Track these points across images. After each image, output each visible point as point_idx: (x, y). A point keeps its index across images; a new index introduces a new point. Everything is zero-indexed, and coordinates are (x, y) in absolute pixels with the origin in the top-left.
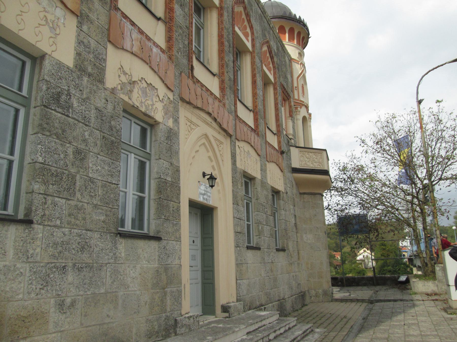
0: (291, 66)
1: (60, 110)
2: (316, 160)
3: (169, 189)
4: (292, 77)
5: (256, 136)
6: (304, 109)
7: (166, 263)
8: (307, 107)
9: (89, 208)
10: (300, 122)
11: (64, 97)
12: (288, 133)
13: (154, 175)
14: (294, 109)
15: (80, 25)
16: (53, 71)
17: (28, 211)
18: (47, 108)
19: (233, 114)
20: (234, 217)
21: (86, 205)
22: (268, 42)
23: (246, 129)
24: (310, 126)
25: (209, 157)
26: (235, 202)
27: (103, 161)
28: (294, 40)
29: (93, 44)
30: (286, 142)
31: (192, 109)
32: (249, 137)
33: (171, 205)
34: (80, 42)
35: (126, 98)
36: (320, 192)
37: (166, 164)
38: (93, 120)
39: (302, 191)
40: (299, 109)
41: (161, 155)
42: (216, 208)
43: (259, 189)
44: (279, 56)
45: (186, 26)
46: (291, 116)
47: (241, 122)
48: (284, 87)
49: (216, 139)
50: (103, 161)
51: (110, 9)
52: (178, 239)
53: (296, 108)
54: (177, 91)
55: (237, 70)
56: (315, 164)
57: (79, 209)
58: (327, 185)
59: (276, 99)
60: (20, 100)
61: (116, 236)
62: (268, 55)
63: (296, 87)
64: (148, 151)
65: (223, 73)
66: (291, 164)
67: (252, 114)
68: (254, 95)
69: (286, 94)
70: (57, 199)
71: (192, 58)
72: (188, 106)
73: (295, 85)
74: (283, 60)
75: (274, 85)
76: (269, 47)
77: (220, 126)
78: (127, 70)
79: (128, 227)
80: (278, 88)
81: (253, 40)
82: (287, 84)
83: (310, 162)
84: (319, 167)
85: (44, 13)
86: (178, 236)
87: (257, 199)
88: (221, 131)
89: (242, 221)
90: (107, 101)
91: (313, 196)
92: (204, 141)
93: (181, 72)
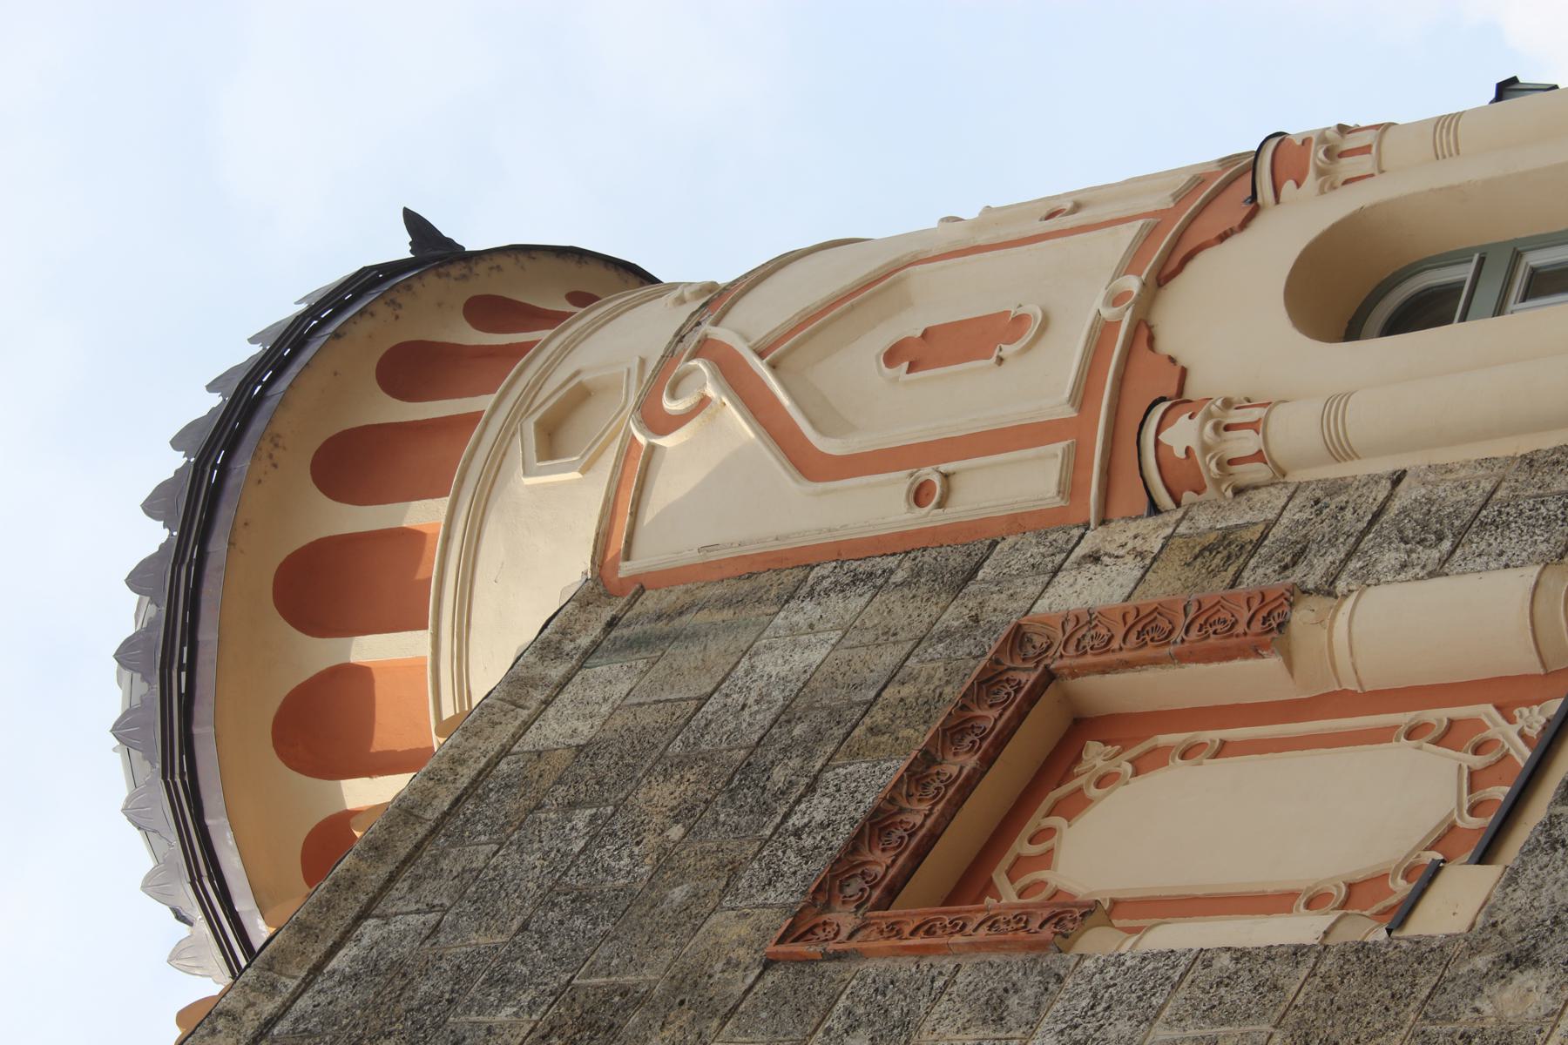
28: (412, 540)
40: (1182, 434)
44: (461, 977)
46: (1269, 627)
48: (845, 866)
53: (1182, 479)
63: (919, 495)
69: (959, 763)
73: (878, 507)
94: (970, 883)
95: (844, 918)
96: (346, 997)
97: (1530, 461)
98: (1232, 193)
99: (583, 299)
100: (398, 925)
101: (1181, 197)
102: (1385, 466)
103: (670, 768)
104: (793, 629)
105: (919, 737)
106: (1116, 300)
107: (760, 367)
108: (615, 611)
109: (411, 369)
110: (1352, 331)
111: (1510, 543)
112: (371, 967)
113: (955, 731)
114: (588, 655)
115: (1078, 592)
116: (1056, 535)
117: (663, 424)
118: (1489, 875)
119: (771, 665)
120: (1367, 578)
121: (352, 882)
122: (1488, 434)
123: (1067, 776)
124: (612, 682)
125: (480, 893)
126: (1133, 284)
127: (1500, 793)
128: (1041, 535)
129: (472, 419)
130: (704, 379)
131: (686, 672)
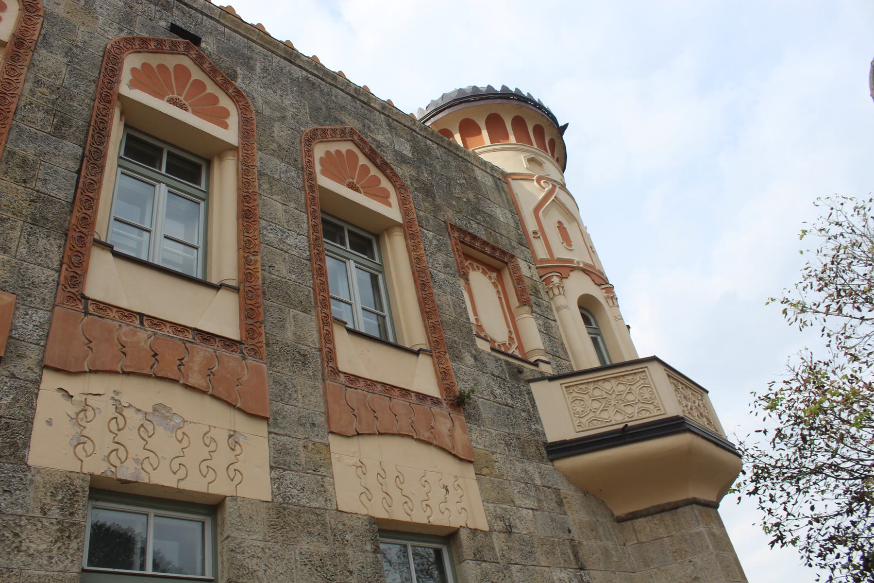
2: (630, 397)
12: (526, 351)
36: (692, 494)
39: (620, 512)
40: (556, 280)
44: (431, 165)
46: (524, 302)
53: (548, 281)
56: (629, 410)
58: (714, 465)
63: (535, 233)
68: (247, 246)
69: (488, 250)
73: (531, 225)
80: (430, 235)
83: (611, 409)
84: (645, 414)
91: (667, 516)
94: (467, 256)
95: (456, 235)
96: (422, 144)
97: (562, 344)
98: (601, 280)
99: (558, 160)
100: (437, 151)
101: (599, 271)
102: (557, 318)
103: (476, 196)
104: (505, 214)
105: (491, 242)
106: (578, 263)
107: (553, 198)
108: (502, 179)
109: (539, 131)
110: (580, 307)
111: (548, 343)
112: (428, 148)
113: (494, 248)
114: (493, 176)
115: (523, 266)
116: (533, 259)
117: (538, 181)
118: (490, 351)
119: (498, 211)
120: (536, 319)
121: (443, 141)
122: (566, 336)
123: (490, 270)
124: (489, 181)
125: (446, 165)
126: (581, 265)
127: (503, 349)
128: (532, 257)
129: (532, 144)
130: (548, 187)
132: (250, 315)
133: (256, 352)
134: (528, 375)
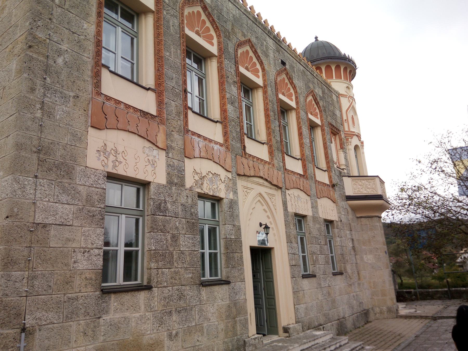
0: (339, 102)
1: (161, 214)
3: (234, 244)
4: (341, 111)
5: (305, 180)
6: (355, 138)
7: (235, 299)
8: (359, 136)
9: (182, 271)
10: (352, 153)
11: (163, 205)
13: (223, 236)
14: (345, 141)
15: (167, 153)
16: (156, 191)
17: (149, 280)
18: (154, 215)
19: (282, 169)
20: (289, 254)
21: (180, 269)
22: (312, 91)
23: (295, 177)
24: (363, 153)
25: (264, 210)
26: (289, 241)
27: (189, 238)
29: (176, 162)
30: (338, 174)
31: (247, 178)
32: (298, 183)
33: (236, 256)
34: (168, 166)
35: (199, 190)
37: (230, 227)
38: (180, 213)
40: (350, 140)
41: (226, 221)
42: (273, 248)
43: (311, 224)
44: (325, 98)
45: (237, 117)
46: (342, 148)
47: (290, 173)
49: (268, 194)
50: (189, 238)
51: (184, 135)
52: (243, 280)
53: (347, 140)
54: (234, 170)
55: (284, 128)
57: (176, 273)
59: (324, 140)
60: (138, 213)
61: (200, 286)
62: (313, 102)
63: (345, 120)
64: (217, 220)
65: (271, 140)
66: (345, 193)
67: (300, 161)
68: (302, 145)
70: (164, 270)
71: (244, 140)
72: (243, 178)
73: (345, 118)
74: (330, 99)
75: (322, 127)
76: (314, 96)
77: (271, 183)
78: (198, 171)
79: (208, 277)
81: (297, 98)
82: (336, 121)
85: (147, 158)
86: (242, 278)
87: (309, 234)
88: (272, 187)
89: (296, 256)
90: (188, 197)
92: (259, 198)
93: (236, 155)
109: (350, 72)
113: (337, 129)
116: (344, 131)
130: (351, 101)
131: (337, 106)
132: (304, 166)
133: (307, 178)
134: (342, 174)
